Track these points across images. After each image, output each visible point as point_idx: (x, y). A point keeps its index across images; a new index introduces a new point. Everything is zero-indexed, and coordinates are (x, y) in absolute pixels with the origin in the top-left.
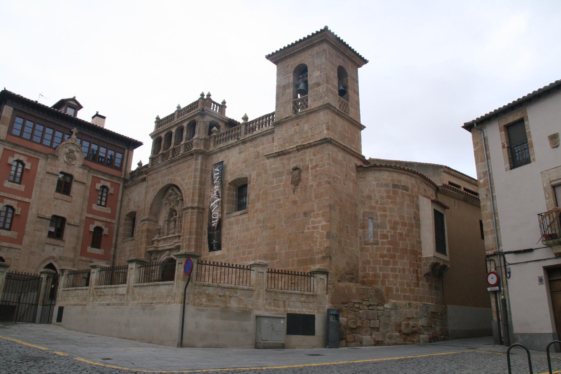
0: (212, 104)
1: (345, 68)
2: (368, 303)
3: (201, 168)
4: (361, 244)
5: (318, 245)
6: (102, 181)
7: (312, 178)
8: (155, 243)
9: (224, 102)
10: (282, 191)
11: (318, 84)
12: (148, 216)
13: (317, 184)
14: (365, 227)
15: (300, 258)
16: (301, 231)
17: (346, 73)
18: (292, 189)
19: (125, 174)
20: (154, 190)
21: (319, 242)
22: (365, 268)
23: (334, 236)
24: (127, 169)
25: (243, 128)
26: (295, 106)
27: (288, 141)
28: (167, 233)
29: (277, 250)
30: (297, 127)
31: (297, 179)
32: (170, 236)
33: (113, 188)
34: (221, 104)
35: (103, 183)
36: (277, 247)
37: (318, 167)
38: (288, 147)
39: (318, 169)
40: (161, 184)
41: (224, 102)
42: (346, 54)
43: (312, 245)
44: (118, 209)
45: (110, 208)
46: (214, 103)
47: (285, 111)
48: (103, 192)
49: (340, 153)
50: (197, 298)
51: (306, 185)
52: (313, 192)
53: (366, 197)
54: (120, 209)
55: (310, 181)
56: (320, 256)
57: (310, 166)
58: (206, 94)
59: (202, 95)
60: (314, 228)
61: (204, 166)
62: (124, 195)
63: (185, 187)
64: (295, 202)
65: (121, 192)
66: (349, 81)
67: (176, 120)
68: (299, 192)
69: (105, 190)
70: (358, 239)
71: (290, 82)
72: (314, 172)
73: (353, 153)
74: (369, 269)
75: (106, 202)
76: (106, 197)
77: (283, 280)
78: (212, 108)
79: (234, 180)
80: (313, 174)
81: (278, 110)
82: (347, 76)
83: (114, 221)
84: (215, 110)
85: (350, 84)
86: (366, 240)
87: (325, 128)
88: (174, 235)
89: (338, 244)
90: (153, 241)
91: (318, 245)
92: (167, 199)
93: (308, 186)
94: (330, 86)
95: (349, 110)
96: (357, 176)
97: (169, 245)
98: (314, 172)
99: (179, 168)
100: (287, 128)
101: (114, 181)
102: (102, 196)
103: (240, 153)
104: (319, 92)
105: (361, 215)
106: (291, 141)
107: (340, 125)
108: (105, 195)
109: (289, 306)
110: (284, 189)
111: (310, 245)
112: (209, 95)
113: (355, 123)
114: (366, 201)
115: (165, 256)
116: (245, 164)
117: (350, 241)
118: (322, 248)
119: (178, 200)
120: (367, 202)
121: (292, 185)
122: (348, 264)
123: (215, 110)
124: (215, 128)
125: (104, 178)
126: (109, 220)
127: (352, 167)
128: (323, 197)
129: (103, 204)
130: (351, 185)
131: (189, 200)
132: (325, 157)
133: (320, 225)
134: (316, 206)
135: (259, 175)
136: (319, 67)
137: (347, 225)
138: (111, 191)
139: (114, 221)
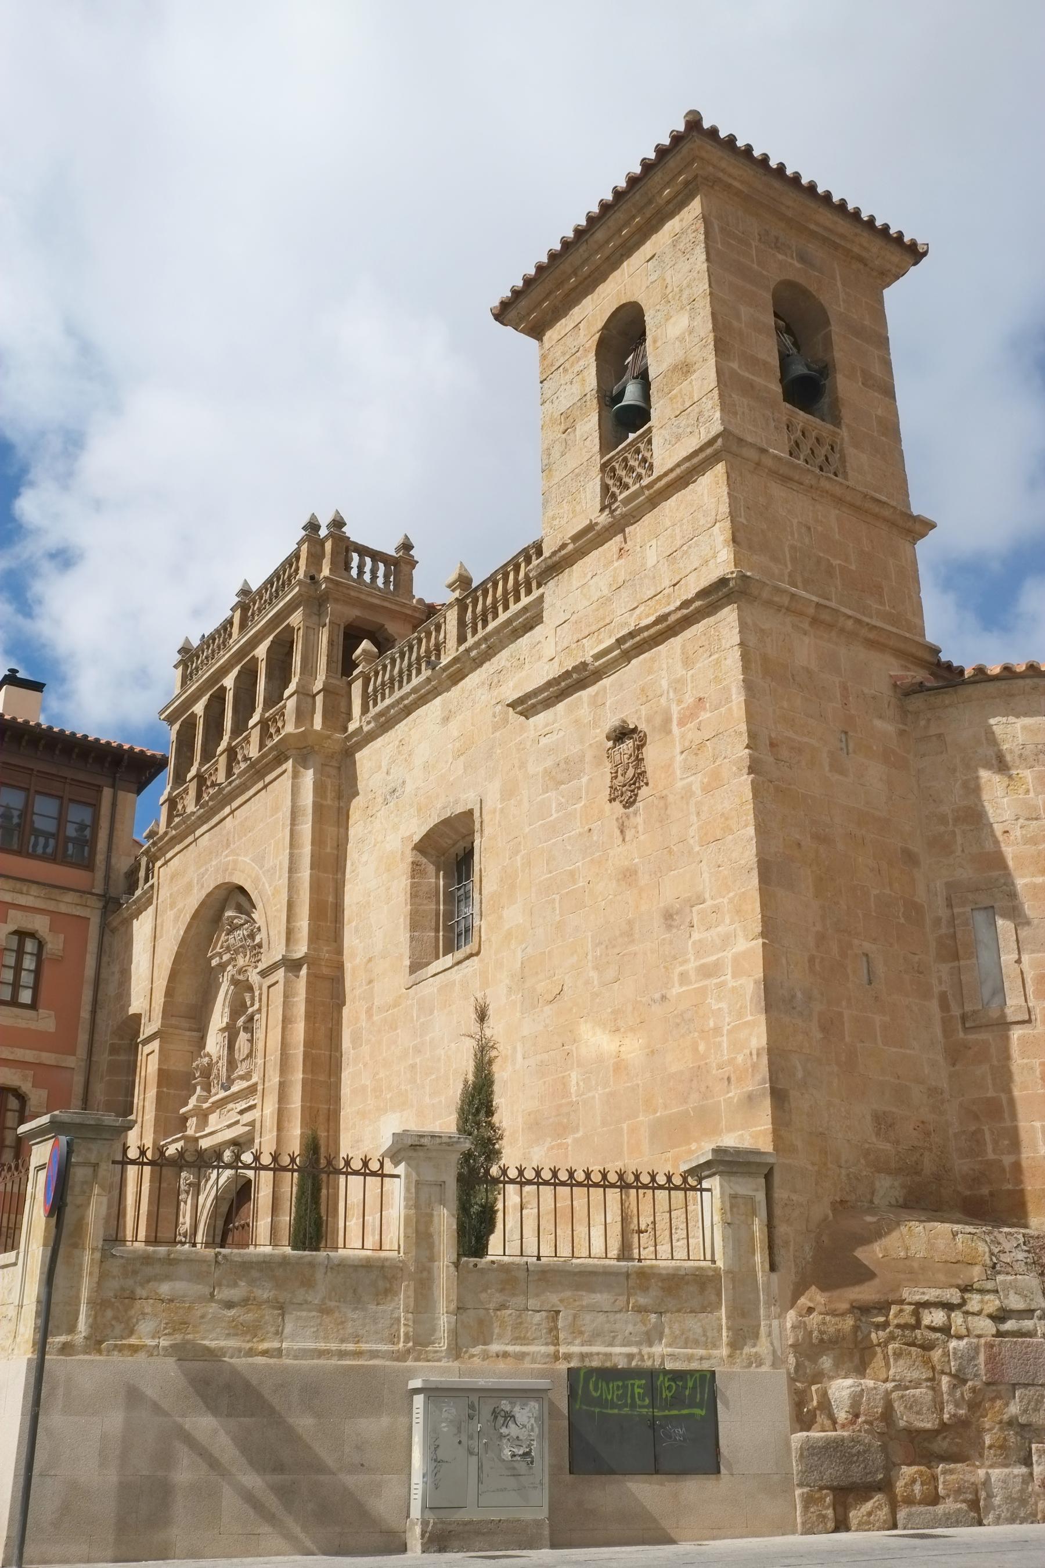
0: (355, 556)
1: (813, 288)
2: (992, 1304)
3: (315, 803)
4: (947, 1031)
5: (725, 1045)
6: (12, 912)
7: (685, 760)
8: (192, 1122)
9: (407, 546)
10: (580, 834)
11: (685, 369)
13: (705, 780)
14: (961, 952)
15: (658, 1114)
16: (657, 996)
17: (823, 312)
18: (615, 822)
19: (107, 878)
20: (177, 918)
21: (729, 1032)
22: (976, 1137)
23: (793, 997)
24: (113, 861)
25: (452, 617)
26: (610, 482)
27: (594, 628)
28: (228, 1077)
29: (573, 1090)
30: (621, 561)
31: (631, 772)
32: (235, 1088)
33: (62, 936)
34: (392, 553)
35: (17, 920)
36: (574, 1076)
37: (705, 709)
38: (588, 651)
39: (704, 716)
41: (407, 546)
42: (812, 227)
43: (702, 1048)
44: (85, 1014)
45: (52, 1013)
46: (363, 551)
47: (574, 511)
48: (20, 953)
49: (806, 640)
50: (115, 1318)
51: (664, 793)
52: (694, 818)
53: (956, 820)
54: (94, 1012)
55: (678, 772)
56: (735, 1093)
57: (675, 710)
58: (324, 521)
59: (313, 526)
60: (707, 972)
61: (330, 794)
62: (105, 959)
63: (267, 885)
64: (628, 876)
65: (92, 946)
66: (834, 337)
67: (237, 640)
68: (640, 828)
69: (30, 946)
70: (934, 1005)
71: (588, 389)
72: (690, 736)
73: (872, 636)
74: (996, 1143)
75: (36, 989)
76: (37, 972)
77: (597, 1218)
78: (354, 573)
79: (431, 830)
80: (687, 744)
81: (550, 514)
82: (827, 322)
83: (70, 1061)
84: (367, 577)
85: (842, 353)
86: (968, 1008)
87: (722, 538)
89: (819, 1035)
90: (185, 1119)
91: (725, 1045)
92: (222, 947)
93: (671, 798)
94: (735, 366)
95: (843, 459)
96: (902, 733)
97: (229, 1126)
98: (690, 736)
100: (585, 575)
101: (63, 908)
102: (18, 969)
103: (446, 720)
104: (691, 397)
105: (940, 901)
106: (602, 624)
107: (795, 521)
108: (29, 963)
109: (576, 1331)
110: (586, 828)
111: (695, 1049)
112: (338, 523)
113: (876, 509)
114: (954, 832)
116: (462, 758)
117: (887, 1019)
118: (740, 1059)
120: (959, 839)
121: (617, 804)
122: (883, 1123)
123: (367, 577)
124: (366, 644)
125: (22, 900)
126: (48, 1058)
127: (874, 698)
128: (731, 832)
129: (26, 996)
130: (875, 773)
132: (729, 662)
133: (728, 954)
134: (706, 875)
135: (509, 792)
136: (684, 296)
137: (867, 946)
138: (54, 945)
139: (70, 1061)
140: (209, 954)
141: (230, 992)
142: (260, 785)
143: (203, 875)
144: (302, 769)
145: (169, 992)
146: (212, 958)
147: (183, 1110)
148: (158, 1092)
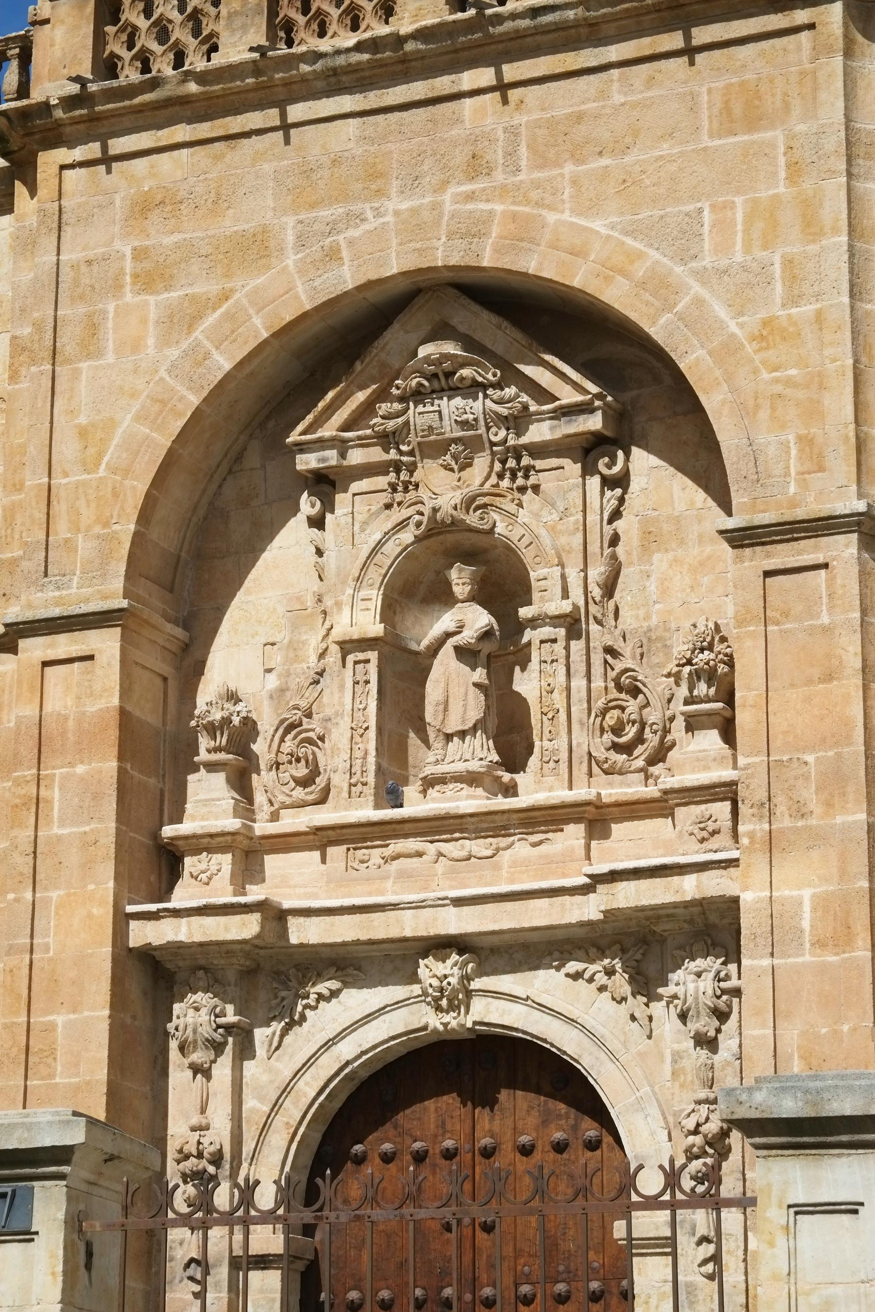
12: (118, 584)
40: (291, 260)
63: (721, 312)
88: (502, 803)
97: (459, 902)
99: (579, 118)
115: (399, 1004)
119: (539, 450)
131: (806, 442)
140: (294, 437)
141: (392, 549)
142: (674, 40)
143: (333, 228)
144: (860, 38)
145: (145, 516)
146: (302, 447)
147: (168, 831)
148: (120, 768)
